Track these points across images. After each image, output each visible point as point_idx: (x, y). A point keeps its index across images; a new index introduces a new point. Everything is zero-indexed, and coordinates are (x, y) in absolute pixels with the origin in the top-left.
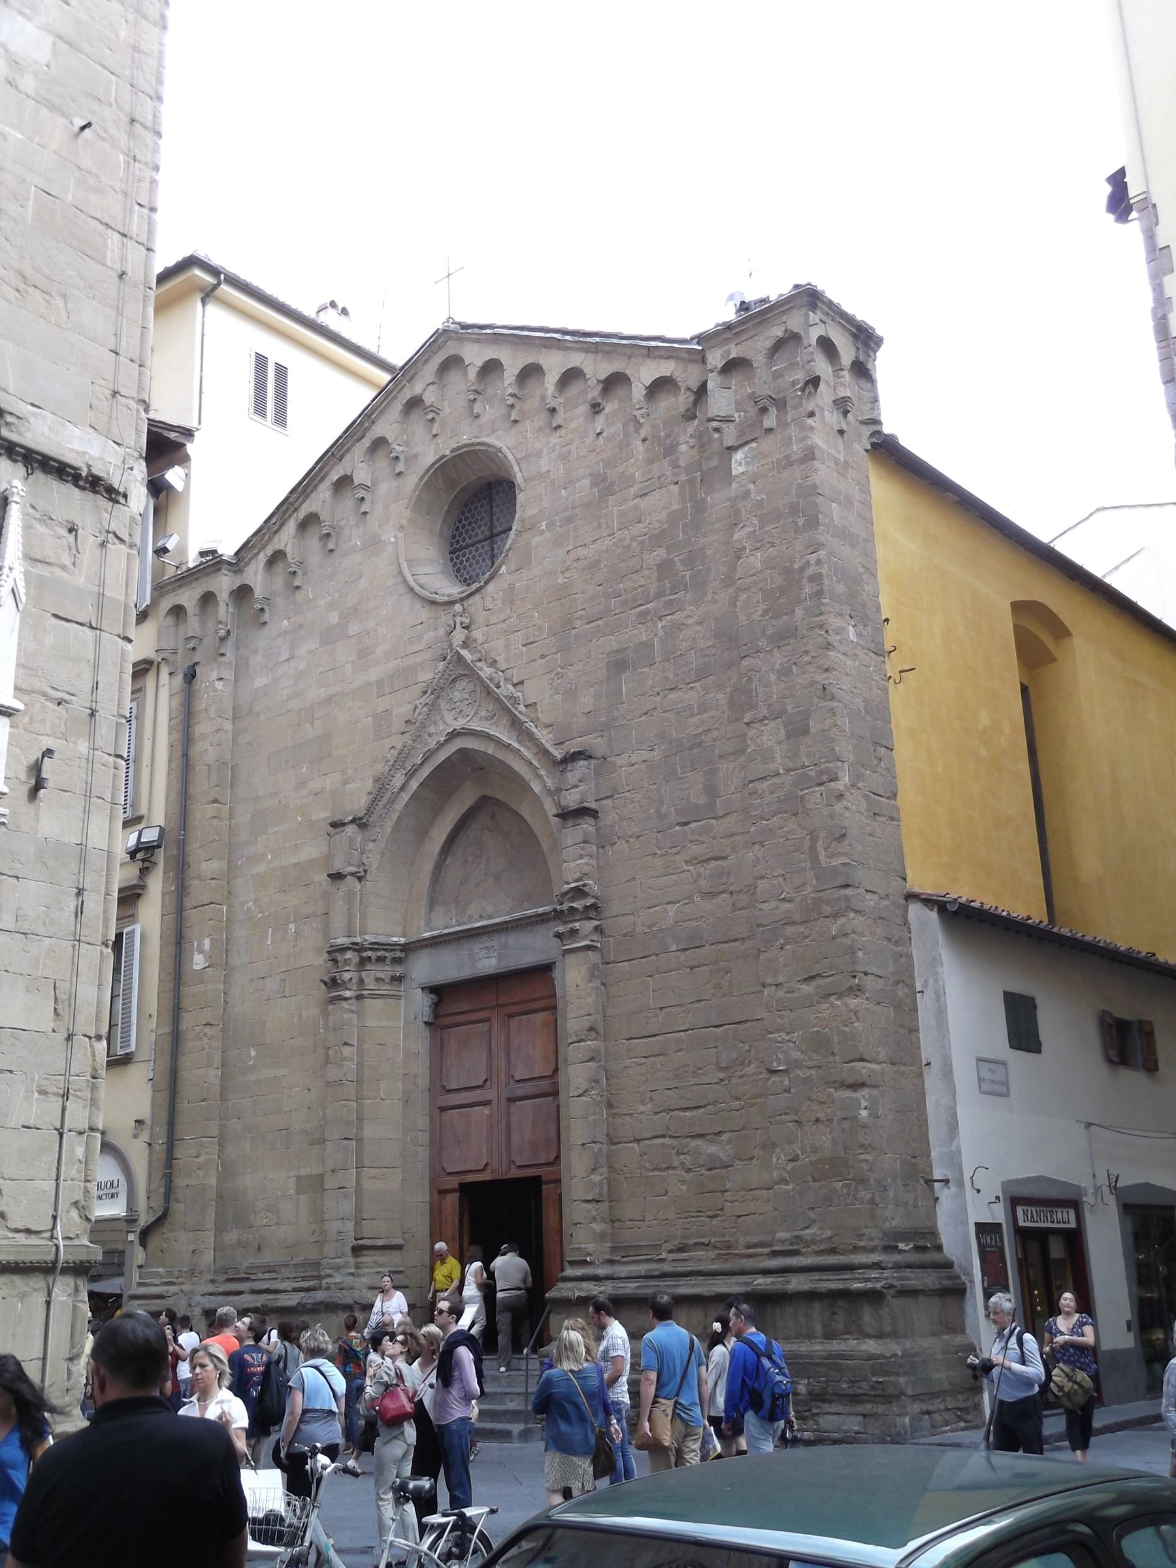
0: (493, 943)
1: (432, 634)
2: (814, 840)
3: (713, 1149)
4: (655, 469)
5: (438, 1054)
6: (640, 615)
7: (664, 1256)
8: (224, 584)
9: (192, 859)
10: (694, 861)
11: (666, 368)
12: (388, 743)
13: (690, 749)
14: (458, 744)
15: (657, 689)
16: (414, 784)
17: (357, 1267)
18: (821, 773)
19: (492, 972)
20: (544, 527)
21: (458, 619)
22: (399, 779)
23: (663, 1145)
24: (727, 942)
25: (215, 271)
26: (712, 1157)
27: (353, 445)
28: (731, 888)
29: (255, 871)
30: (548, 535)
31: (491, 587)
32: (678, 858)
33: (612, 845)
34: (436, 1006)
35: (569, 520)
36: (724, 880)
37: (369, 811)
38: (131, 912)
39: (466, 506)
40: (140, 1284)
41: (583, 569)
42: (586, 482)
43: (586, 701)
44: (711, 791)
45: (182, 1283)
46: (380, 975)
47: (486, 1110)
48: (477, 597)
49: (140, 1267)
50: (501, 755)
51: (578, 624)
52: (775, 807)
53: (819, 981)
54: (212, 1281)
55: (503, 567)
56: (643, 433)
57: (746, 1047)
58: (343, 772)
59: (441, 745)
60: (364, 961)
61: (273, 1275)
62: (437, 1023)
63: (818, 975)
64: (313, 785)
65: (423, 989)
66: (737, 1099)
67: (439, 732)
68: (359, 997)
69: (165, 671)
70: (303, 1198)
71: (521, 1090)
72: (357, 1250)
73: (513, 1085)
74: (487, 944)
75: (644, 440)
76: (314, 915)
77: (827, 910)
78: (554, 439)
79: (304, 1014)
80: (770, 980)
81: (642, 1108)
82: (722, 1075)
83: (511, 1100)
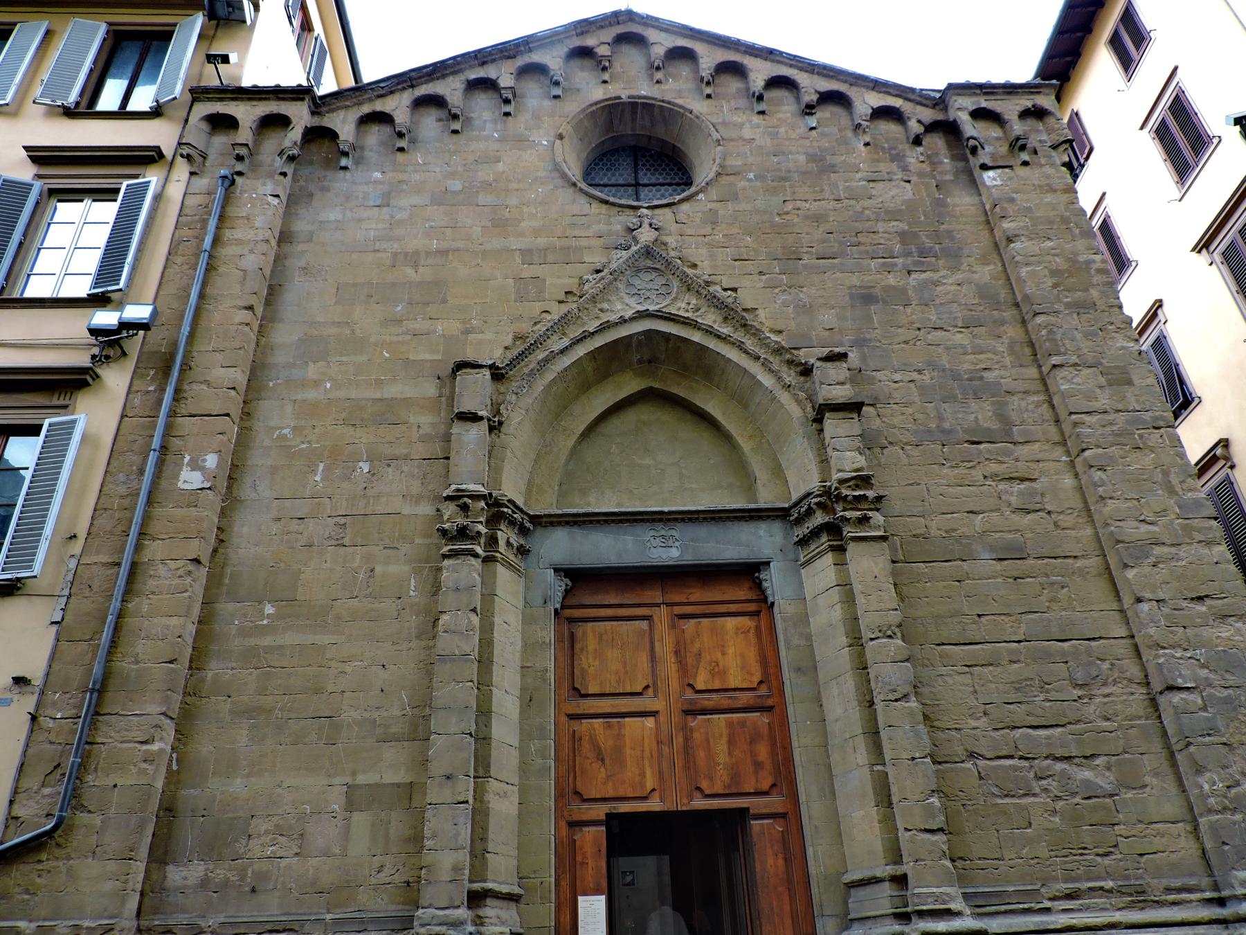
0: (673, 532)
1: (602, 227)
2: (1166, 473)
3: (1087, 774)
5: (569, 645)
6: (884, 264)
7: (1047, 904)
8: (300, 115)
9: (198, 360)
10: (994, 476)
11: (897, 102)
12: (538, 307)
13: (970, 379)
15: (917, 325)
16: (581, 351)
18: (1157, 418)
19: (671, 563)
20: (751, 176)
21: (646, 221)
22: (557, 344)
23: (1015, 768)
24: (1055, 558)
26: (1087, 782)
27: (501, 58)
28: (1049, 508)
29: (299, 397)
30: (758, 184)
31: (685, 207)
32: (973, 472)
33: (883, 448)
36: (1038, 499)
37: (511, 364)
38: (66, 402)
39: (604, 155)
41: (807, 217)
42: (802, 158)
43: (827, 318)
44: (1002, 417)
47: (650, 722)
48: (667, 211)
50: (712, 344)
51: (805, 257)
52: (1111, 438)
53: (1208, 602)
55: (701, 196)
57: (1106, 665)
58: (464, 322)
59: (623, 321)
63: (1207, 596)
64: (420, 325)
65: (556, 570)
68: (486, 560)
70: (361, 820)
72: (476, 899)
73: (690, 695)
74: (663, 533)
75: (867, 144)
76: (406, 458)
77: (1198, 536)
78: (757, 119)
80: (1148, 595)
81: (974, 723)
82: (1080, 693)
83: (691, 712)
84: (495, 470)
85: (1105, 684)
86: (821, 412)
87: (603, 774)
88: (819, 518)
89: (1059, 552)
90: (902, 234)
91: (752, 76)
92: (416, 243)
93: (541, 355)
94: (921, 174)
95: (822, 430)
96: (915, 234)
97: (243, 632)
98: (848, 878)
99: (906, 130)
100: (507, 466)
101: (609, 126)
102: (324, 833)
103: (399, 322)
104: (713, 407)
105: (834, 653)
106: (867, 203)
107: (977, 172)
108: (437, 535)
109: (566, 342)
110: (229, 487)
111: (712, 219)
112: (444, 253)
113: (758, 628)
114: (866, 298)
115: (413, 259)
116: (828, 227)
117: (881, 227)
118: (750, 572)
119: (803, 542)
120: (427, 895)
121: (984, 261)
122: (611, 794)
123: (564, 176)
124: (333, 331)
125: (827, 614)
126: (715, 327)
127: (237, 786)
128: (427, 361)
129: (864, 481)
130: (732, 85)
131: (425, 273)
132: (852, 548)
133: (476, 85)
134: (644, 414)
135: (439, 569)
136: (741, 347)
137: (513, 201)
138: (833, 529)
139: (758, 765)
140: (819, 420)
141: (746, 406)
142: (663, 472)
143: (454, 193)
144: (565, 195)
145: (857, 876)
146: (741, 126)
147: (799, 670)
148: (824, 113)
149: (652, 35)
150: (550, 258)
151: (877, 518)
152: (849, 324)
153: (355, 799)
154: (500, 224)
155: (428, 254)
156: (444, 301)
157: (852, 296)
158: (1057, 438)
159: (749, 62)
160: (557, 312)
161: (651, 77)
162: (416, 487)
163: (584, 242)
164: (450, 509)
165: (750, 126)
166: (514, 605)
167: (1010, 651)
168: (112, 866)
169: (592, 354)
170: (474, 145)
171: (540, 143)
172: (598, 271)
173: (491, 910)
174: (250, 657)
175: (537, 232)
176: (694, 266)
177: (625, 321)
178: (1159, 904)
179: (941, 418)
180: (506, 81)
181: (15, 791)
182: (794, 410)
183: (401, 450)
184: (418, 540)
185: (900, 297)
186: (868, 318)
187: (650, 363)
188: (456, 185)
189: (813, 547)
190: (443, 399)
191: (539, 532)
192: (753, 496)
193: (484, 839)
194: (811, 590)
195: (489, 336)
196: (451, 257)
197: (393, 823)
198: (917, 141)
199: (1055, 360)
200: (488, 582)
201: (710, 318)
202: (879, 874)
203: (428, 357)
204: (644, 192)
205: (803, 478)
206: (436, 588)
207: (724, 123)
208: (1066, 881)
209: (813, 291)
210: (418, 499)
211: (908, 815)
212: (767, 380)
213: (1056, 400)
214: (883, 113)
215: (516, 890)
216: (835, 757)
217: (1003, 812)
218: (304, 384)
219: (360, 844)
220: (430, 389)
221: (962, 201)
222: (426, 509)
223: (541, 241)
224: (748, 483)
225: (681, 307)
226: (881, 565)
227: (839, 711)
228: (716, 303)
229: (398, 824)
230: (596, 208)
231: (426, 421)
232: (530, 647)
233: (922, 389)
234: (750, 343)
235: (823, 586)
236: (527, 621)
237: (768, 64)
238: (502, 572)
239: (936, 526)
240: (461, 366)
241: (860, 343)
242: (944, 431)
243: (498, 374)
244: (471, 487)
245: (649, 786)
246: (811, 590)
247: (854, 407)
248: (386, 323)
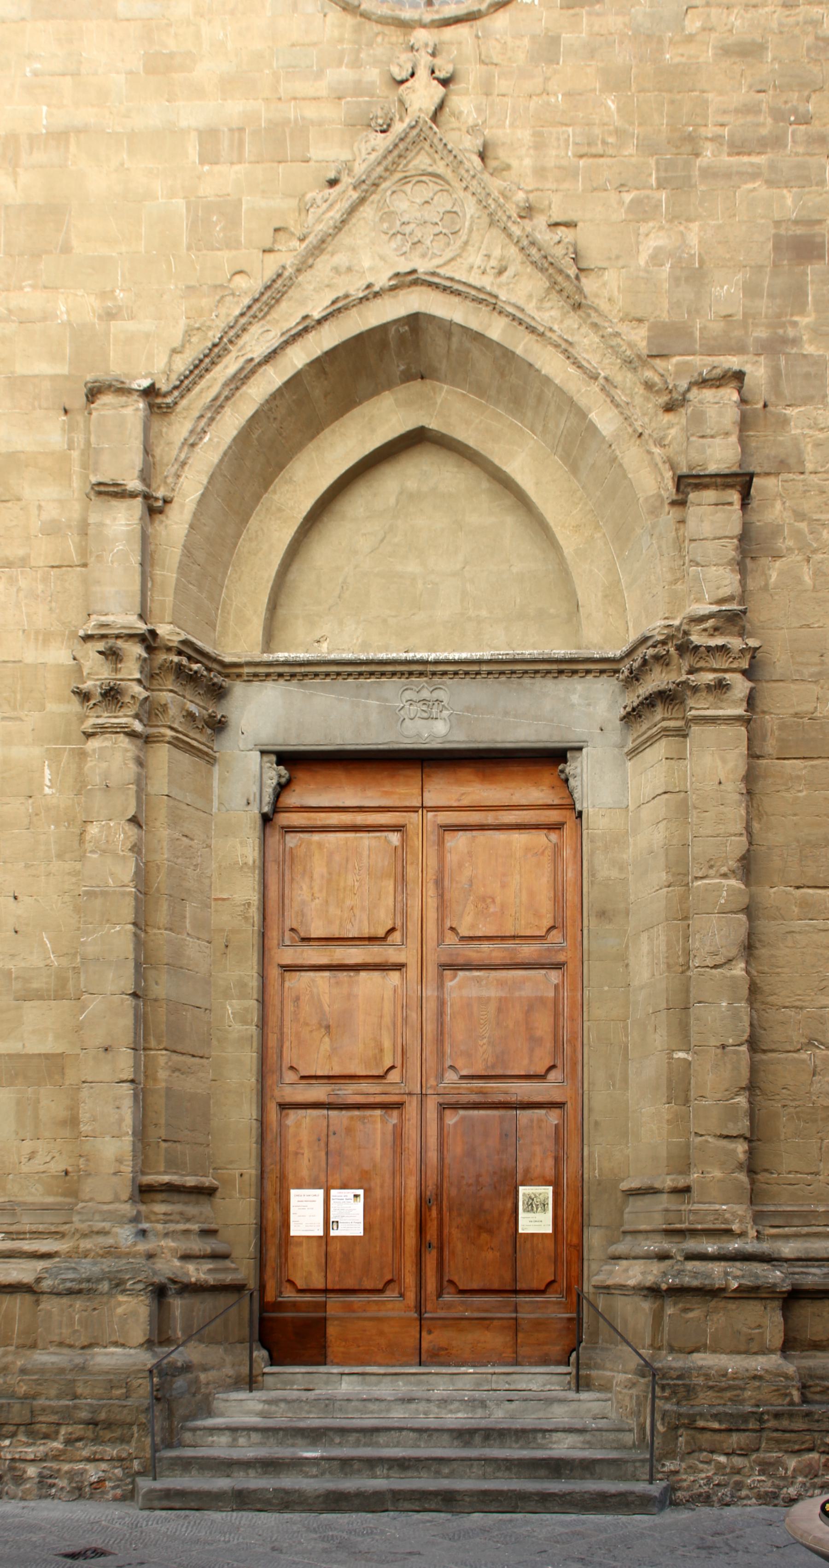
16: (298, 358)
22: (257, 342)
43: (725, 292)
46: (193, 708)
50: (522, 345)
58: (104, 295)
93: (229, 366)
95: (682, 522)
108: (75, 699)
109: (273, 340)
113: (557, 850)
118: (552, 758)
122: (337, 1071)
126: (531, 308)
128: (45, 377)
135: (82, 755)
139: (534, 1041)
140: (680, 503)
145: (635, 1184)
155: (33, 139)
156: (66, 249)
157: (776, 248)
163: (311, 112)
164: (91, 655)
172: (333, 183)
177: (376, 295)
184: (52, 707)
186: (796, 297)
189: (645, 727)
190: (75, 454)
195: (147, 325)
196: (73, 148)
197: (44, 1102)
201: (523, 290)
202: (658, 1185)
203: (44, 368)
210: (45, 638)
222: (59, 655)
223: (235, 108)
226: (731, 765)
227: (646, 975)
234: (587, 344)
245: (388, 1063)
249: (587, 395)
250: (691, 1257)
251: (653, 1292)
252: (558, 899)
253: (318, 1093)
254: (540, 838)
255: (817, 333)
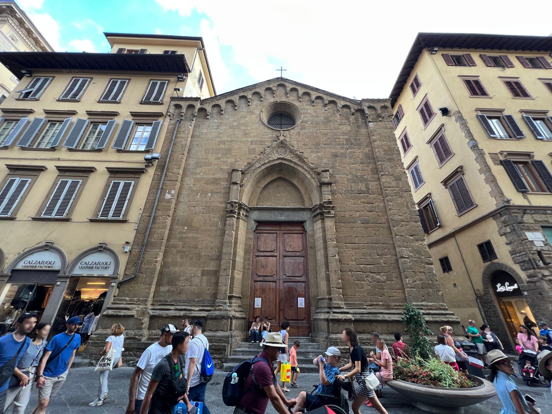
2: (407, 203)
3: (379, 277)
4: (343, 121)
8: (198, 105)
10: (364, 203)
11: (348, 104)
12: (254, 156)
14: (280, 161)
16: (263, 167)
17: (230, 303)
22: (257, 165)
23: (361, 274)
25: (203, 47)
29: (195, 177)
31: (292, 131)
34: (257, 226)
35: (317, 124)
40: (113, 303)
42: (323, 118)
43: (325, 161)
45: (140, 304)
47: (275, 258)
49: (114, 296)
54: (152, 305)
56: (340, 113)
59: (274, 160)
60: (239, 209)
61: (186, 304)
62: (256, 231)
66: (385, 264)
67: (275, 156)
69: (168, 119)
70: (205, 278)
71: (288, 254)
72: (230, 298)
76: (220, 192)
78: (312, 108)
79: (212, 219)
83: (285, 256)
84: (241, 197)
85: (386, 255)
86: (322, 184)
87: (263, 270)
88: (318, 211)
89: (378, 222)
90: (346, 139)
91: (312, 96)
92: (224, 139)
94: (353, 123)
96: (350, 139)
97: (179, 233)
98: (318, 298)
99: (351, 111)
100: (244, 195)
101: (275, 109)
102: (196, 281)
103: (219, 159)
104: (295, 182)
105: (320, 244)
106: (338, 131)
107: (368, 123)
109: (260, 165)
110: (177, 198)
111: (299, 133)
112: (232, 141)
113: (302, 238)
114: (335, 156)
115: (224, 142)
116: (327, 137)
117: (341, 137)
118: (301, 223)
119: (315, 216)
120: (219, 296)
121: (367, 146)
122: (264, 275)
123: (262, 122)
124: (204, 160)
125: (319, 234)
127: (177, 269)
129: (330, 203)
130: (307, 98)
131: (227, 146)
132: (326, 219)
133: (241, 97)
134: (279, 183)
135: (226, 220)
136: (303, 168)
137: (249, 128)
138: (322, 214)
140: (321, 187)
141: (303, 182)
142: (282, 199)
143: (235, 126)
144: (262, 127)
145: (320, 297)
146: (308, 109)
147: (311, 248)
148: (329, 106)
149: (287, 84)
150: (258, 143)
151: (333, 212)
152: (331, 162)
153: (203, 273)
154: (246, 134)
158: (380, 193)
159: (311, 92)
160: (258, 157)
161: (286, 96)
162: (222, 200)
163: (266, 139)
164: (229, 206)
165: (310, 110)
166: (242, 230)
167: (363, 246)
168: (147, 286)
169: (266, 168)
170: (240, 113)
171: (260, 111)
173: (233, 301)
174: (181, 239)
175: (254, 137)
176: (293, 146)
178: (393, 309)
179: (351, 187)
180: (250, 96)
181: (126, 268)
182: (315, 183)
183: (218, 191)
185: (344, 155)
187: (281, 171)
188: (235, 124)
191: (251, 212)
192: (304, 204)
193: (233, 284)
194: (315, 228)
198: (353, 114)
199: (382, 173)
200: (238, 223)
201: (296, 160)
204: (283, 126)
205: (316, 201)
206: (225, 224)
207: (304, 109)
208: (371, 302)
209: (322, 154)
210: (222, 203)
211: (333, 284)
212: (309, 176)
213: (381, 183)
214: (345, 106)
215: (240, 296)
216: (318, 269)
217: (357, 284)
218: (196, 174)
219: (204, 284)
220: (227, 176)
221: (363, 131)
222: (223, 205)
223: (256, 139)
224: (303, 202)
225: (288, 157)
227: (320, 258)
228: (297, 156)
229: (213, 279)
230: (270, 131)
231: (224, 184)
232: (247, 239)
233: (347, 179)
234: (305, 167)
235: (318, 228)
236: (247, 232)
237: (316, 93)
238: (241, 221)
239: (347, 214)
240: (233, 170)
241: (333, 167)
242: (352, 191)
243: (243, 173)
244: (235, 200)
246: (315, 228)
247: (329, 184)
248: (216, 159)
249: (306, 173)
250: (334, 313)
251: (327, 320)
252: (303, 246)
253: (261, 279)
254: (300, 235)
255: (339, 166)
